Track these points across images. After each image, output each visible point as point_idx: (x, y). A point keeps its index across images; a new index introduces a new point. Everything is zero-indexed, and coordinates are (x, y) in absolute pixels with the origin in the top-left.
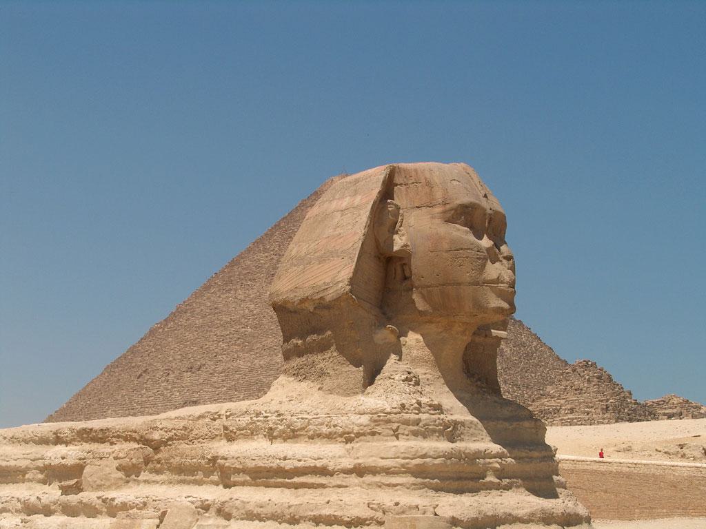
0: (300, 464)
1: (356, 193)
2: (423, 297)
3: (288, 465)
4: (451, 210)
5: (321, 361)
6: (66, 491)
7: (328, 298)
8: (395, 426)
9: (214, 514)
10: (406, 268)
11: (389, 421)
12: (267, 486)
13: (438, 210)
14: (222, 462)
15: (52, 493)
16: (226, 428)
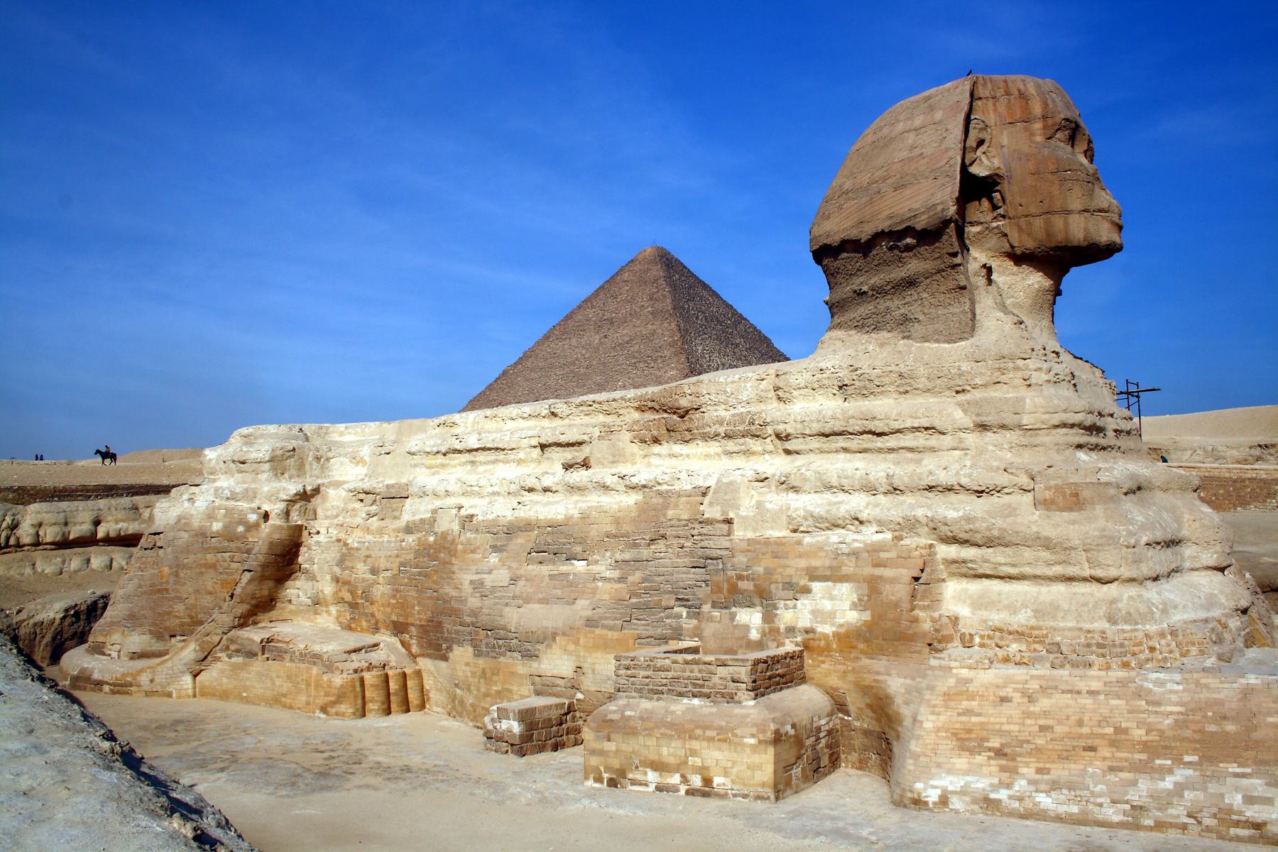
0: (897, 425)
1: (932, 109)
2: (1020, 230)
3: (879, 426)
4: (1054, 125)
5: (896, 305)
6: (568, 467)
7: (919, 227)
8: (1026, 374)
9: (774, 488)
10: (997, 195)
11: (1017, 369)
12: (845, 450)
13: (1038, 126)
14: (781, 427)
15: (552, 470)
16: (777, 389)
